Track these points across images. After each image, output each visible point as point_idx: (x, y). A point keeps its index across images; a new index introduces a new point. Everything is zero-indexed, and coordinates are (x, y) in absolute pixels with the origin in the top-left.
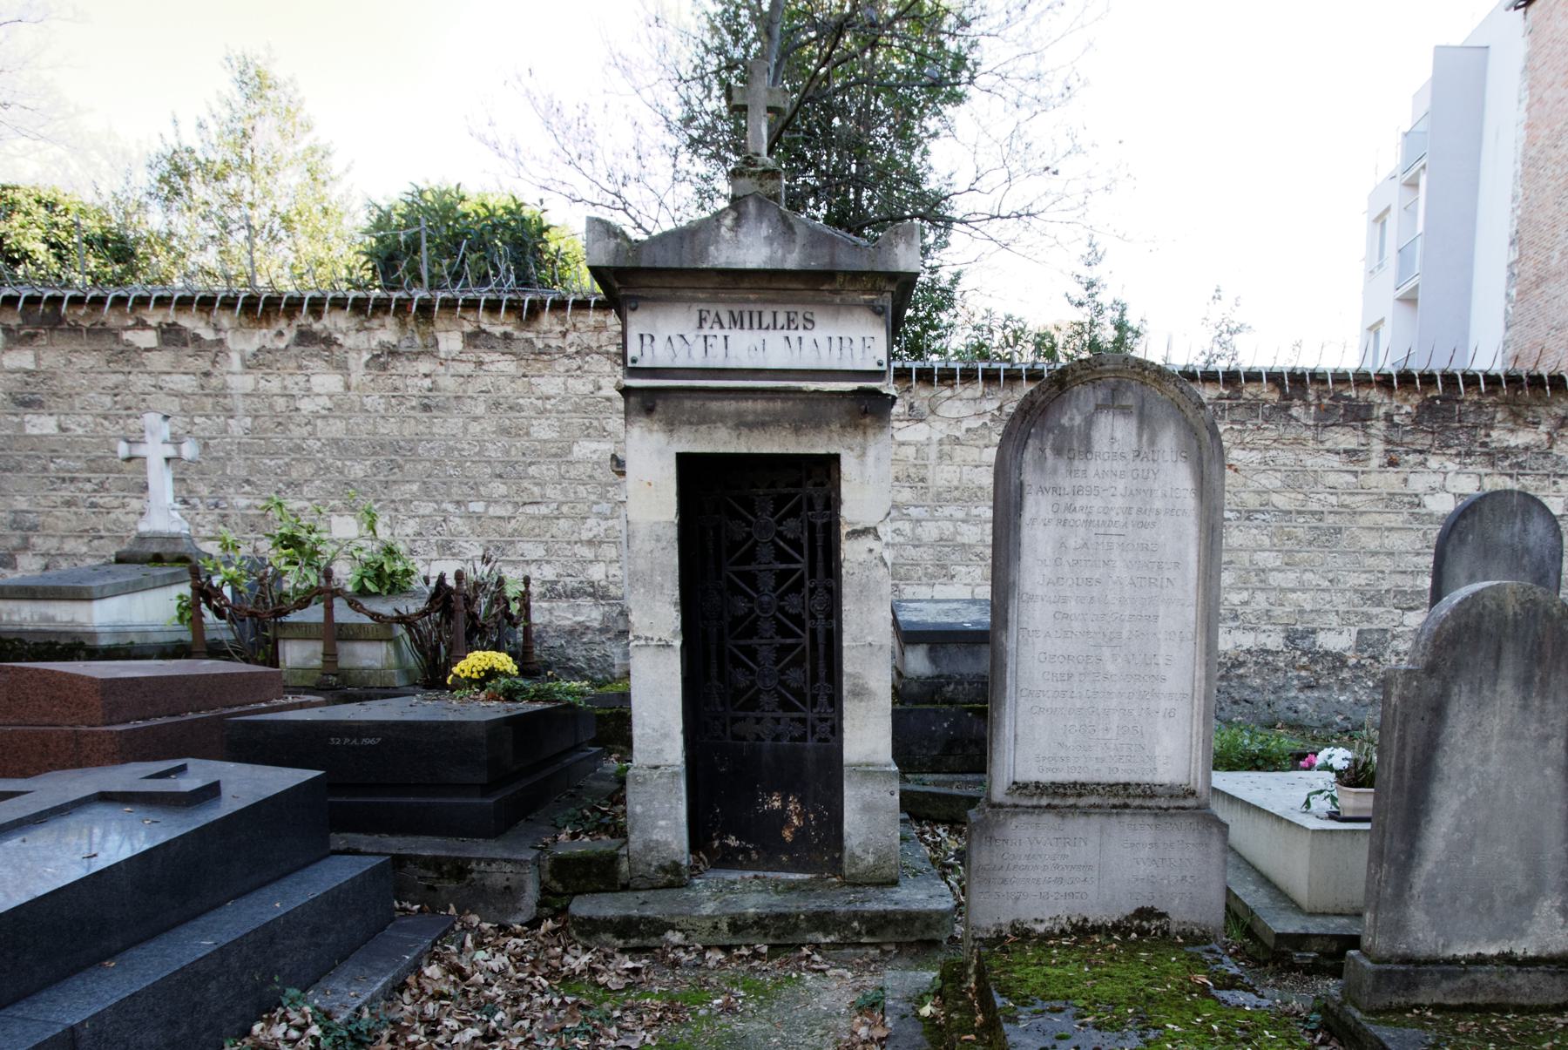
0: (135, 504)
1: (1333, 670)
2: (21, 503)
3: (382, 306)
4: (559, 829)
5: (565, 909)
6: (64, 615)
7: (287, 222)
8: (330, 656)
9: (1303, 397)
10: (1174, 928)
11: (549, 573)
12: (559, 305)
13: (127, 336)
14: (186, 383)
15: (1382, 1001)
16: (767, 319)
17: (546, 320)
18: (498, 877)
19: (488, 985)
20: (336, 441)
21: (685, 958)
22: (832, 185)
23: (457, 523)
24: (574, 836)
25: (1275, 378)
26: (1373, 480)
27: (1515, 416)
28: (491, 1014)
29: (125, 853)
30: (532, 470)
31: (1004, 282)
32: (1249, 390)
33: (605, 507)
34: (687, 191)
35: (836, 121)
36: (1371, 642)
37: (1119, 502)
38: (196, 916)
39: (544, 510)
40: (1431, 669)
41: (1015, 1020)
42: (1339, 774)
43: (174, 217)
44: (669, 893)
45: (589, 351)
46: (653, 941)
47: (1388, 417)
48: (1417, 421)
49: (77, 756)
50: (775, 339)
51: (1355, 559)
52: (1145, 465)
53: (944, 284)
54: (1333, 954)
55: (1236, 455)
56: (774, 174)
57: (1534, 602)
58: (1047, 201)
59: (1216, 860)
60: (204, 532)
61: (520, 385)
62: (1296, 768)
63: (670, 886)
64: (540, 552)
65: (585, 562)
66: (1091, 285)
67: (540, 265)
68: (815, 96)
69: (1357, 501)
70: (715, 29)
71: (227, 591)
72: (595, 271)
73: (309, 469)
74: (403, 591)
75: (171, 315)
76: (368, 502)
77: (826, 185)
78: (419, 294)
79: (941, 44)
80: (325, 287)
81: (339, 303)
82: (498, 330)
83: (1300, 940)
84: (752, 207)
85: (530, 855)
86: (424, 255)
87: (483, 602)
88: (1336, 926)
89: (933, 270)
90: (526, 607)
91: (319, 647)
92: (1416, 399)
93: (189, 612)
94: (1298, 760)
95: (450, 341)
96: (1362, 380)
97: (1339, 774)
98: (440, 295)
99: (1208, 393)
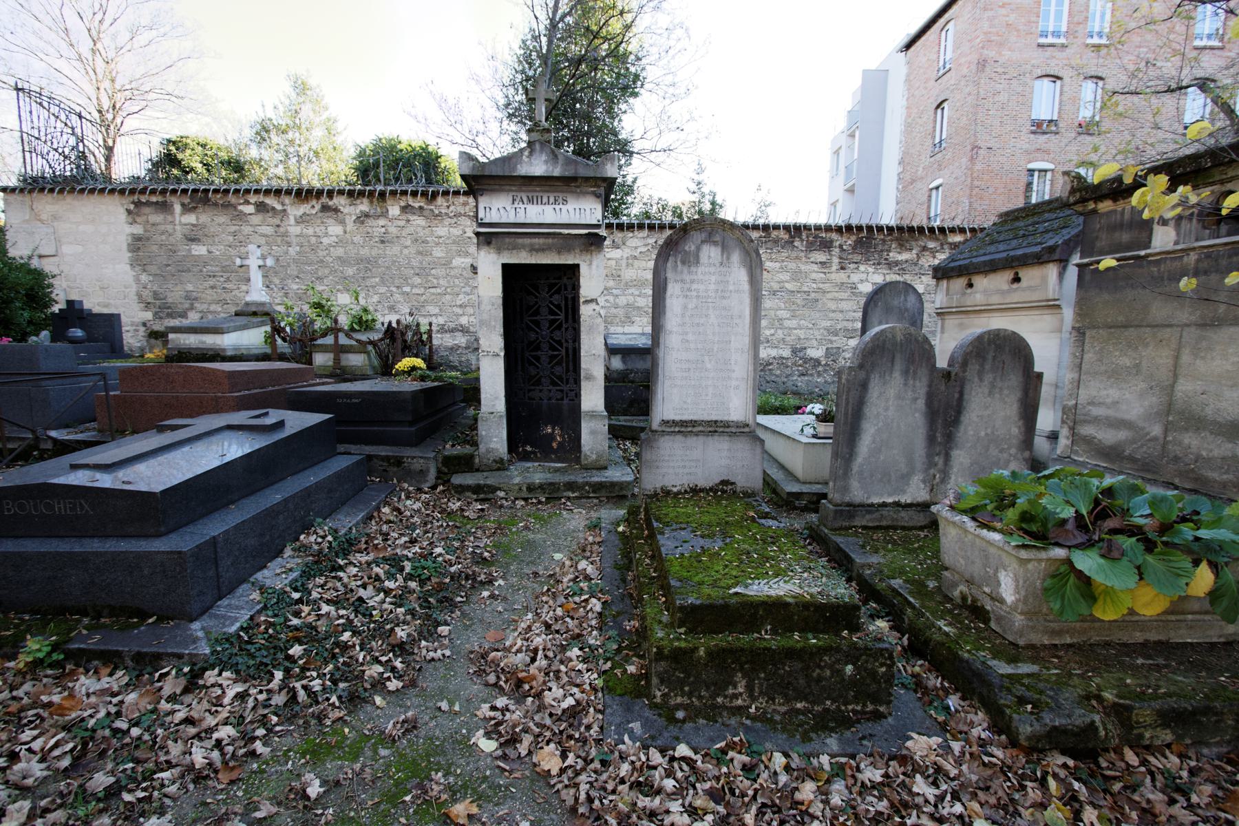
0: (244, 288)
1: (814, 367)
2: (190, 287)
3: (361, 194)
4: (446, 443)
5: (449, 481)
6: (210, 340)
7: (316, 154)
8: (337, 360)
9: (800, 237)
10: (738, 490)
11: (441, 320)
12: (446, 193)
13: (240, 207)
14: (268, 230)
15: (837, 525)
16: (545, 200)
17: (440, 200)
18: (417, 465)
19: (412, 516)
20: (340, 258)
21: (506, 504)
22: (576, 136)
23: (397, 297)
24: (453, 446)
25: (787, 228)
26: (833, 276)
27: (901, 246)
28: (414, 531)
29: (240, 454)
30: (433, 272)
31: (658, 182)
32: (774, 234)
33: (468, 289)
34: (507, 139)
35: (578, 106)
36: (832, 354)
37: (712, 287)
38: (272, 484)
39: (439, 291)
40: (861, 366)
41: (663, 533)
42: (817, 416)
43: (263, 151)
44: (498, 473)
45: (460, 215)
46: (491, 496)
47: (841, 246)
48: (854, 248)
49: (217, 407)
50: (549, 209)
51: (824, 314)
52: (724, 269)
53: (629, 183)
54: (814, 502)
55: (768, 265)
56: (548, 131)
57: (910, 334)
58: (678, 144)
59: (758, 457)
60: (277, 301)
61: (427, 231)
62: (797, 413)
63: (499, 469)
64: (437, 311)
65: (458, 315)
66: (699, 183)
67: (437, 174)
68: (568, 93)
69: (826, 286)
70: (520, 62)
71: (288, 329)
72: (463, 177)
73: (327, 271)
74: (372, 329)
75: (261, 198)
76: (355, 287)
77: (573, 136)
78: (379, 188)
79: (627, 69)
80: (335, 184)
81: (341, 192)
82: (417, 205)
83: (798, 495)
84: (538, 146)
85: (432, 455)
86: (382, 169)
87: (410, 334)
88: (816, 488)
89: (624, 176)
90: (430, 337)
91: (331, 356)
92: (854, 238)
93: (270, 339)
94: (797, 410)
95: (394, 210)
96: (828, 228)
97: (817, 416)
98: (389, 188)
99: (755, 235)
